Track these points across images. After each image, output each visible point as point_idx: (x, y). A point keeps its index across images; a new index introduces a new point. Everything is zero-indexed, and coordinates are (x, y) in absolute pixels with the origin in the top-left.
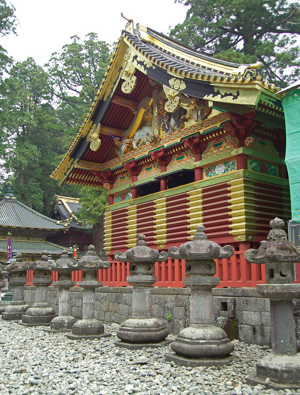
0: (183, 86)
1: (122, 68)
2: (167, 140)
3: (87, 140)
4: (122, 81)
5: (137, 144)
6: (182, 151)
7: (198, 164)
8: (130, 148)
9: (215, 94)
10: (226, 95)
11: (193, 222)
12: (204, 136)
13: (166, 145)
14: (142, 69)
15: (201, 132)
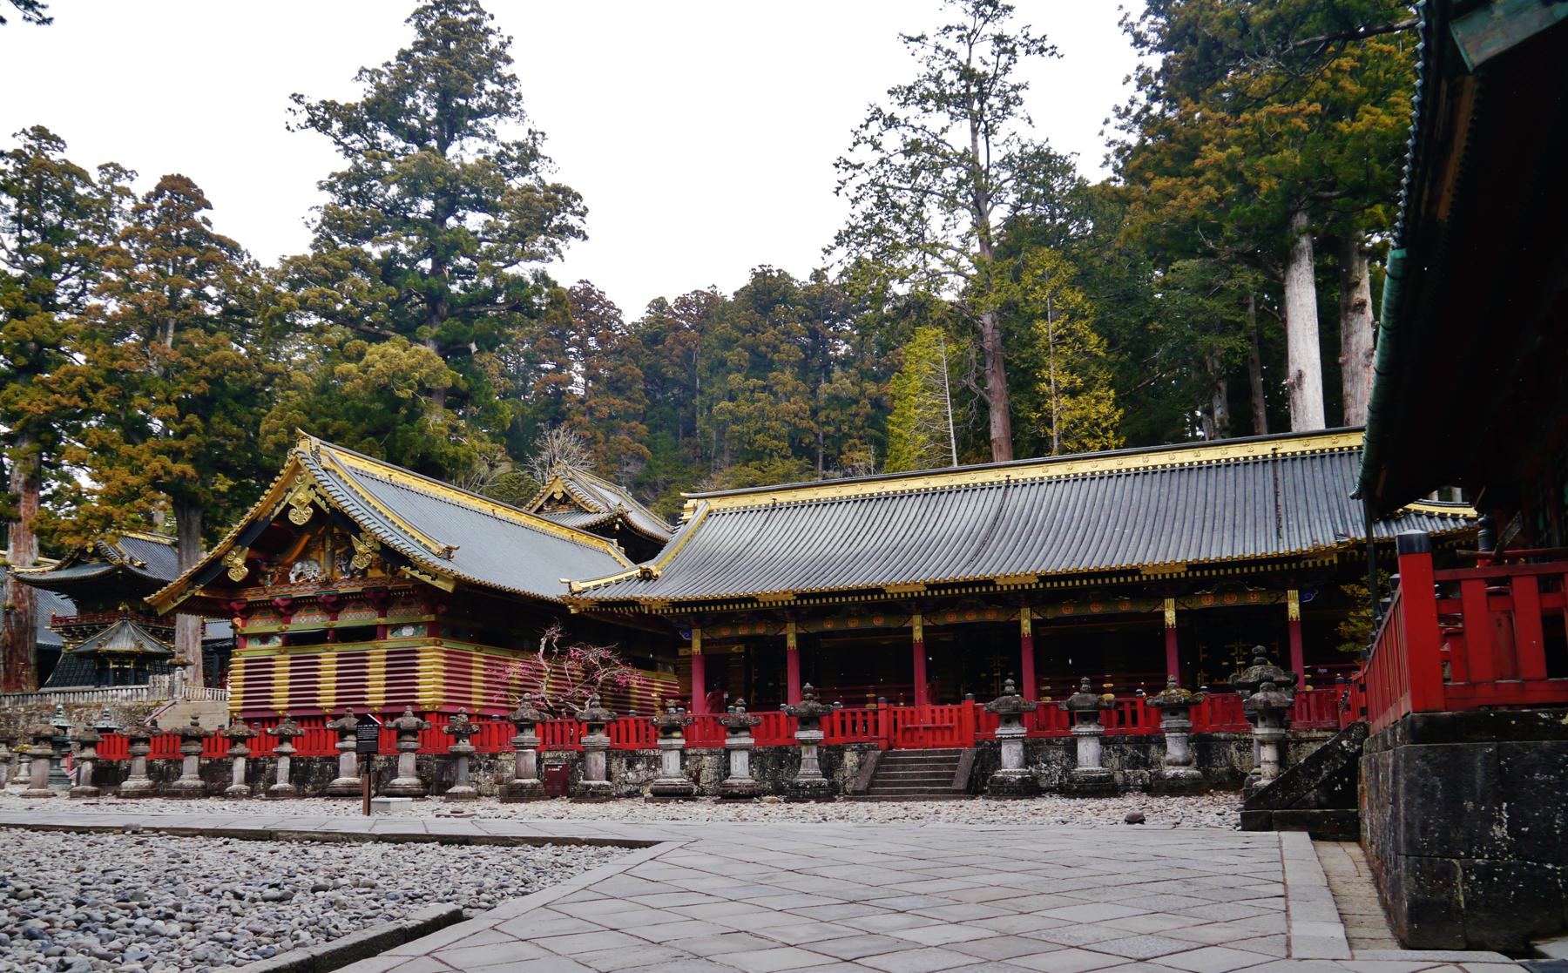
0: (378, 548)
1: (290, 490)
2: (344, 584)
3: (223, 564)
4: (289, 507)
5: (297, 578)
6: (361, 599)
7: (382, 621)
8: (284, 579)
9: (414, 568)
10: (424, 573)
11: (373, 686)
12: (392, 591)
13: (341, 591)
14: (323, 505)
15: (390, 587)
